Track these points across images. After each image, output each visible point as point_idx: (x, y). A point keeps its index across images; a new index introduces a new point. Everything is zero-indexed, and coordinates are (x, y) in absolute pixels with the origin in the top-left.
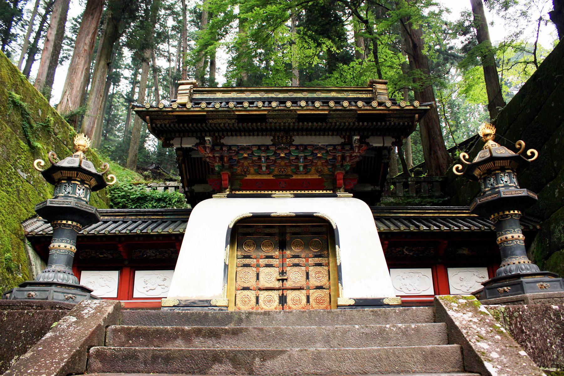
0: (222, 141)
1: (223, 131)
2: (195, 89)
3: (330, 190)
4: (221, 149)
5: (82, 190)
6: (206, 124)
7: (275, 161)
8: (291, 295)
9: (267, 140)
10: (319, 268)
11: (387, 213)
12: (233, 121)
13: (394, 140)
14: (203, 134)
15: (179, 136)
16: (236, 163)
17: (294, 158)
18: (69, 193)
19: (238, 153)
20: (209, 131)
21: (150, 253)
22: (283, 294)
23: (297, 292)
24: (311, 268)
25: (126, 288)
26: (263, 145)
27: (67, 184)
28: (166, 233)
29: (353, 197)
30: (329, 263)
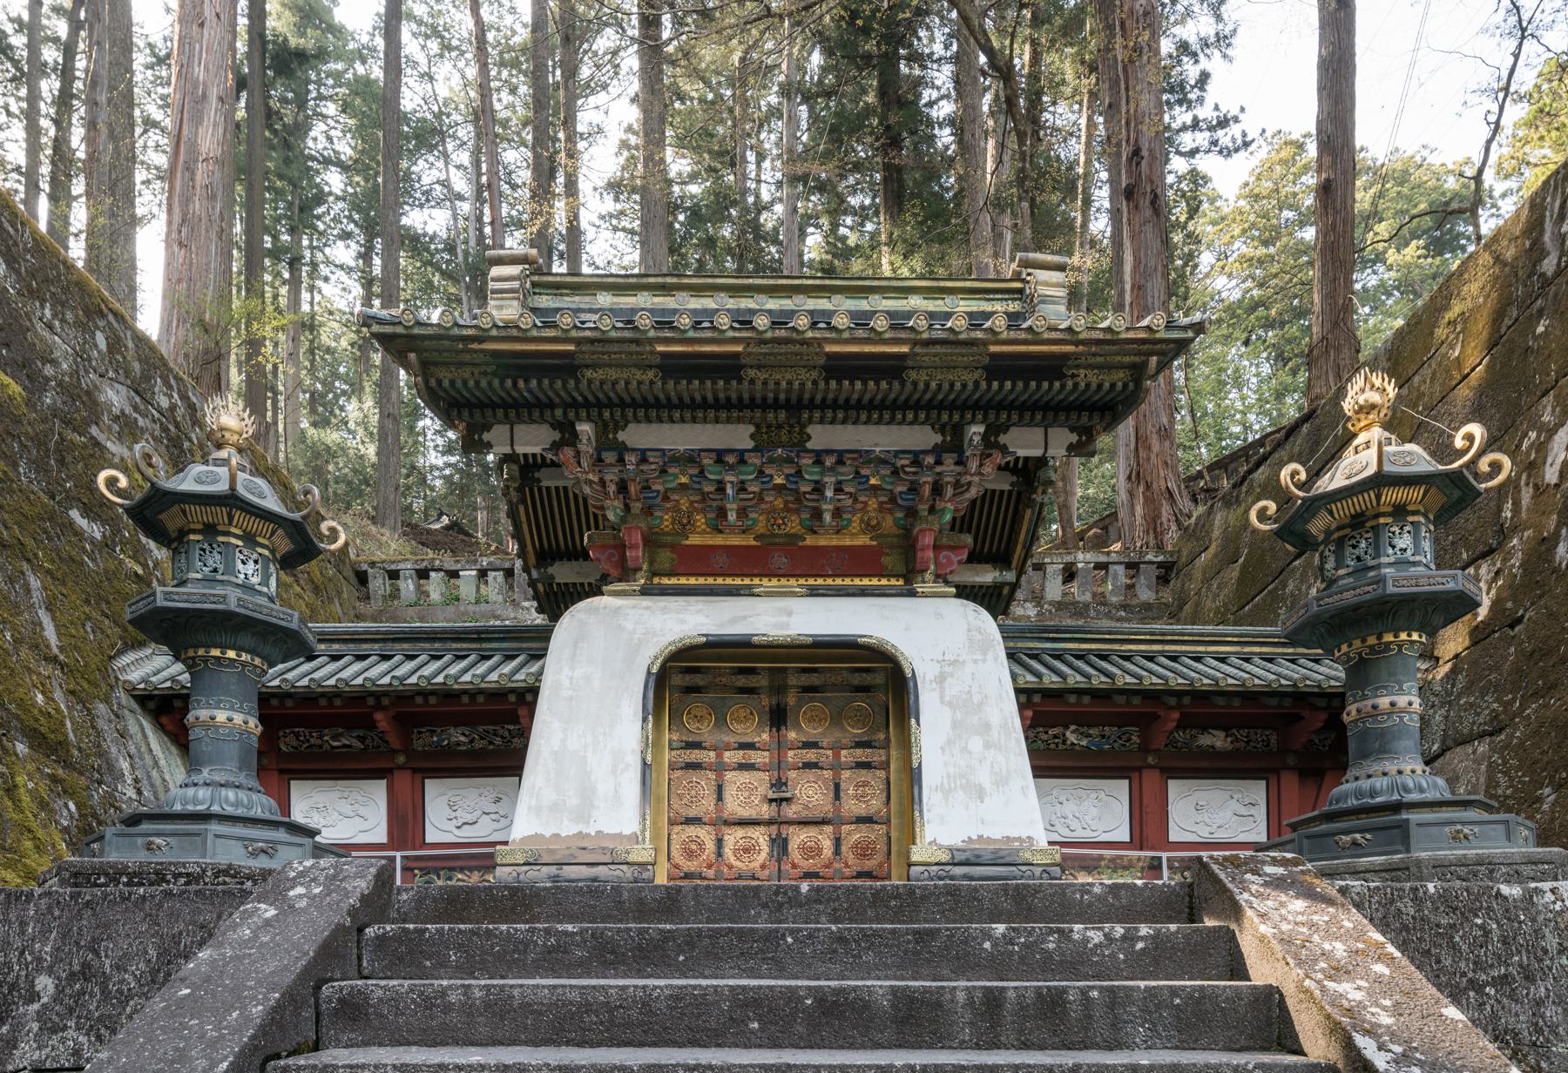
0: (621, 436)
1: (623, 404)
4: (621, 460)
5: (251, 565)
6: (578, 381)
7: (760, 497)
8: (798, 838)
9: (739, 436)
13: (1074, 438)
14: (571, 415)
18: (215, 570)
19: (664, 471)
23: (812, 832)
24: (846, 774)
25: (406, 822)
27: (206, 546)
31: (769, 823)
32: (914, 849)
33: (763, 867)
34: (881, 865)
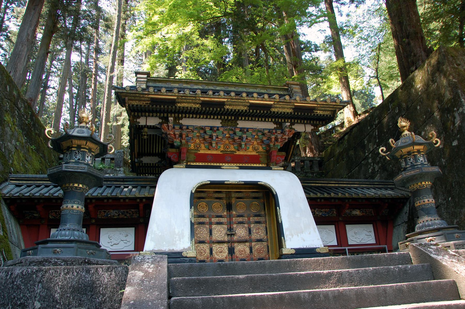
9: (217, 123)
21: (113, 213)
28: (133, 196)
29: (284, 170)
31: (228, 242)
32: (283, 249)
33: (226, 258)
34: (266, 256)
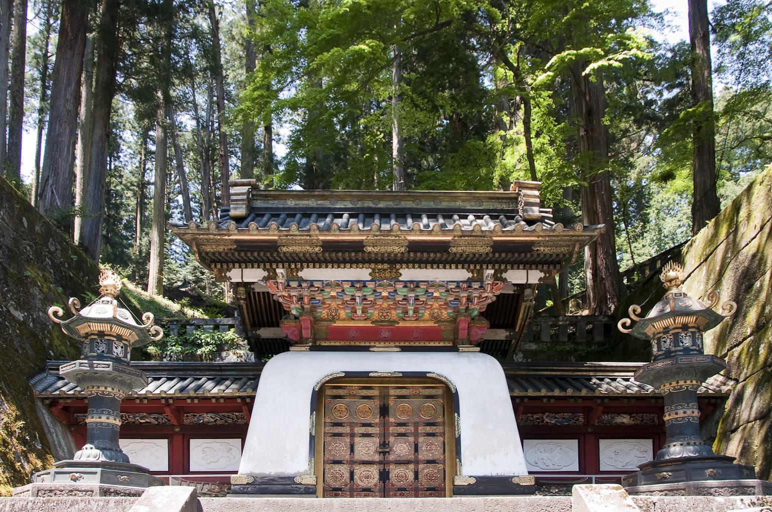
0: (300, 274)
2: (255, 193)
3: (449, 341)
4: (300, 285)
7: (373, 303)
9: (363, 273)
10: (431, 439)
11: (524, 370)
12: (317, 249)
15: (240, 267)
16: (320, 304)
17: (401, 299)
20: (282, 262)
22: (384, 469)
26: (358, 281)
30: (444, 433)
33: (375, 485)
